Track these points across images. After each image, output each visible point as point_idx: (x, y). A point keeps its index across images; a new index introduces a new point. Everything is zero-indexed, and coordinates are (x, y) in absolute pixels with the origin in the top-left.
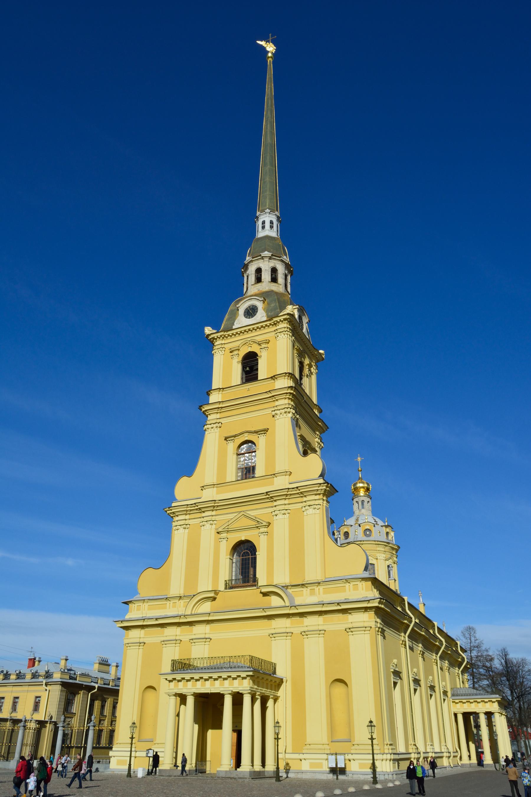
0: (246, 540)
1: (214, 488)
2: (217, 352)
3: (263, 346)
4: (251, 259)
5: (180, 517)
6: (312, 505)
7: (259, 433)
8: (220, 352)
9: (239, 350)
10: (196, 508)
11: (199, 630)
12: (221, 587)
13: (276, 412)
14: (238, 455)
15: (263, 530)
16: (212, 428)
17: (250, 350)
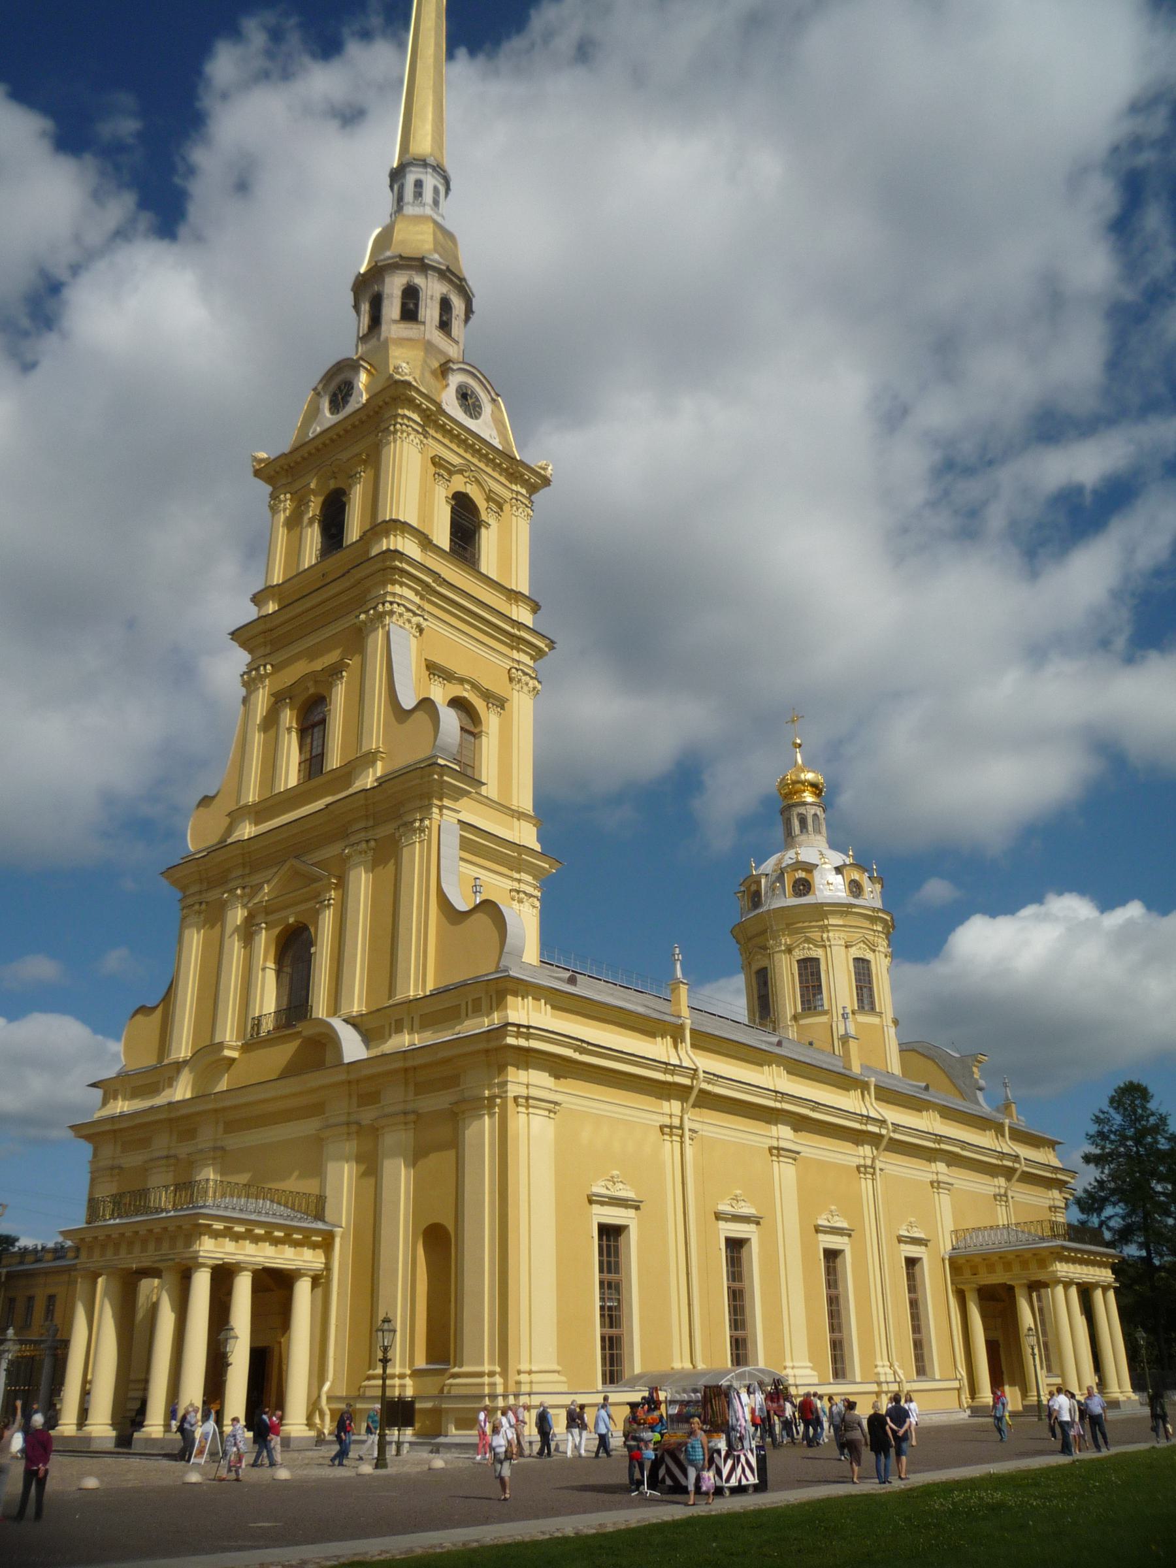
7: (491, 700)
16: (409, 621)
17: (468, 491)
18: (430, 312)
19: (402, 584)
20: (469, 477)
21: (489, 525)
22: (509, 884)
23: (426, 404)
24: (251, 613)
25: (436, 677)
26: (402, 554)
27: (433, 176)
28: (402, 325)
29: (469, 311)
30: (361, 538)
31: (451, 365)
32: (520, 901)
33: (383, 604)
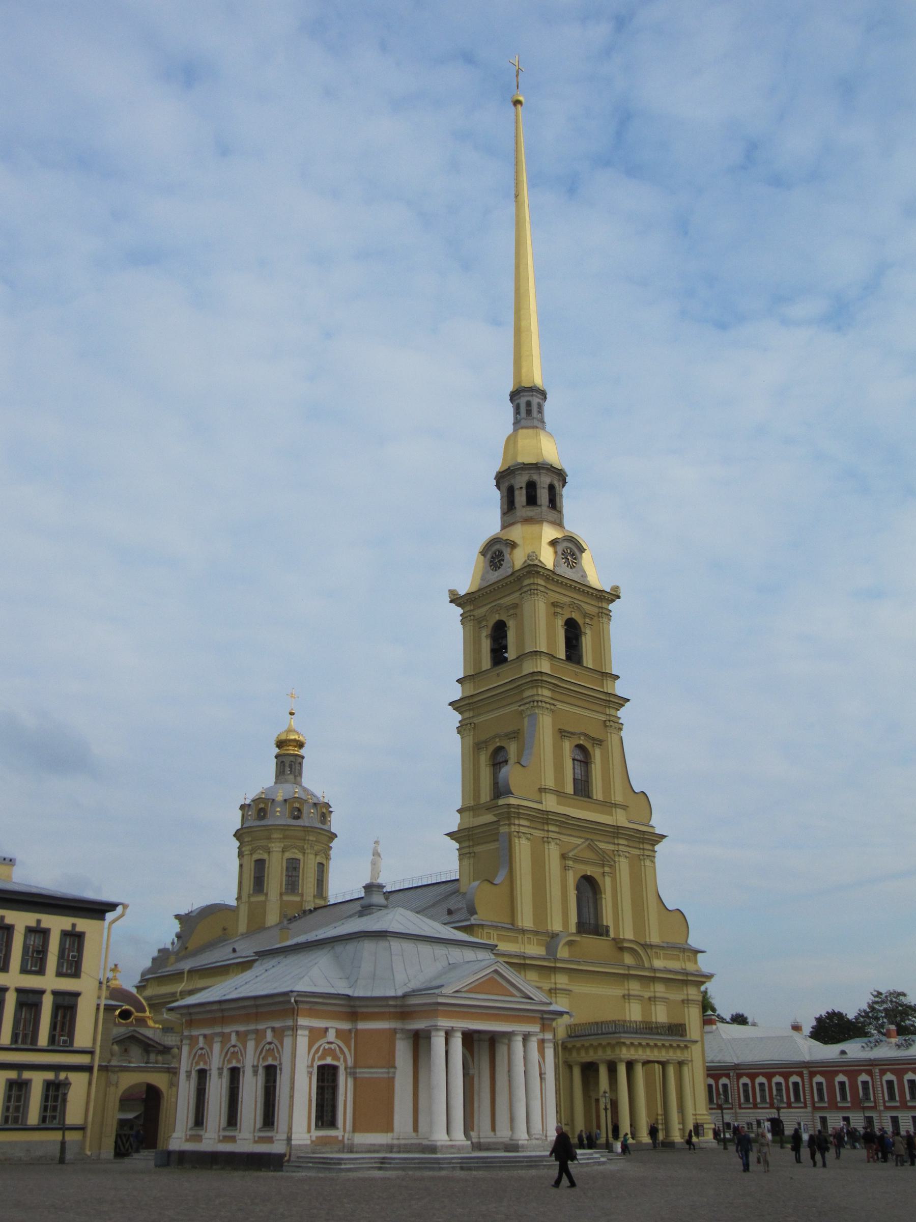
0: (590, 876)
1: (554, 794)
2: (539, 596)
3: (587, 621)
4: (549, 467)
5: (523, 822)
6: (650, 856)
8: (542, 597)
9: (564, 607)
10: (545, 816)
11: (562, 980)
12: (573, 929)
13: (612, 723)
14: (574, 760)
15: (607, 869)
17: (573, 616)
18: (543, 496)
19: (542, 687)
20: (573, 608)
21: (586, 634)
22: (612, 847)
23: (547, 572)
24: (457, 693)
25: (566, 738)
26: (541, 672)
27: (536, 396)
28: (529, 508)
29: (564, 482)
30: (517, 658)
31: (558, 540)
32: (619, 855)
33: (533, 702)
